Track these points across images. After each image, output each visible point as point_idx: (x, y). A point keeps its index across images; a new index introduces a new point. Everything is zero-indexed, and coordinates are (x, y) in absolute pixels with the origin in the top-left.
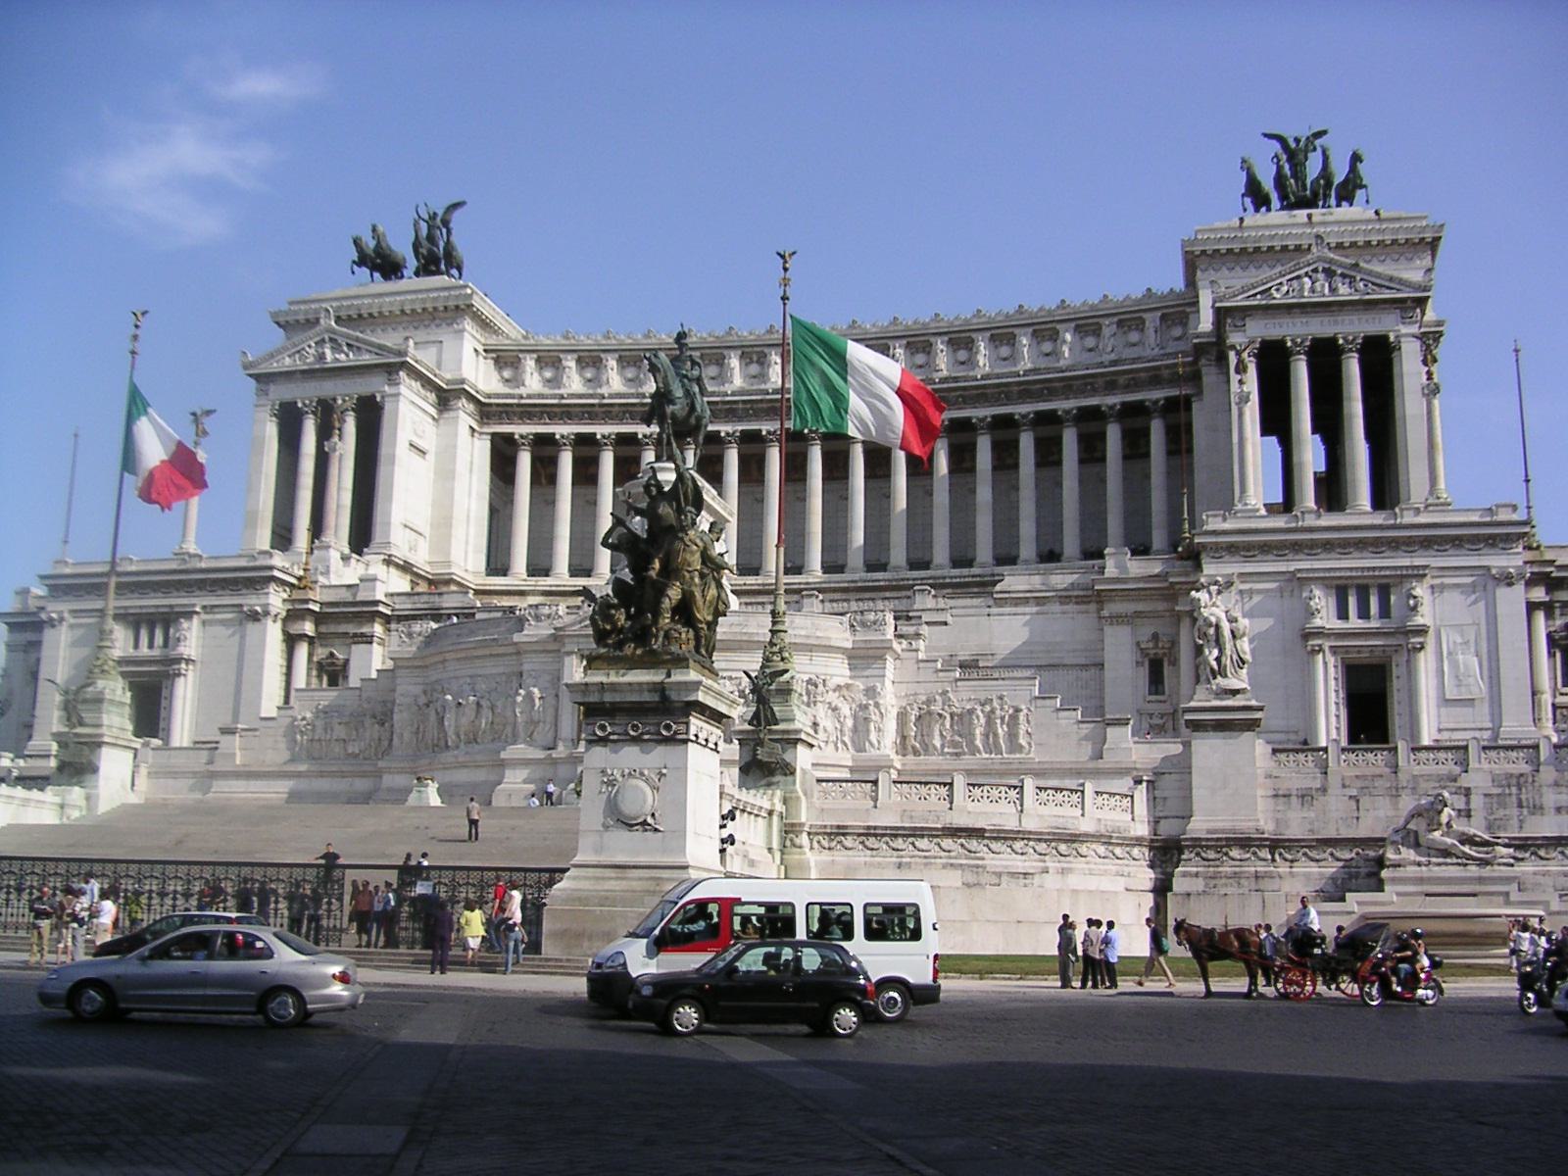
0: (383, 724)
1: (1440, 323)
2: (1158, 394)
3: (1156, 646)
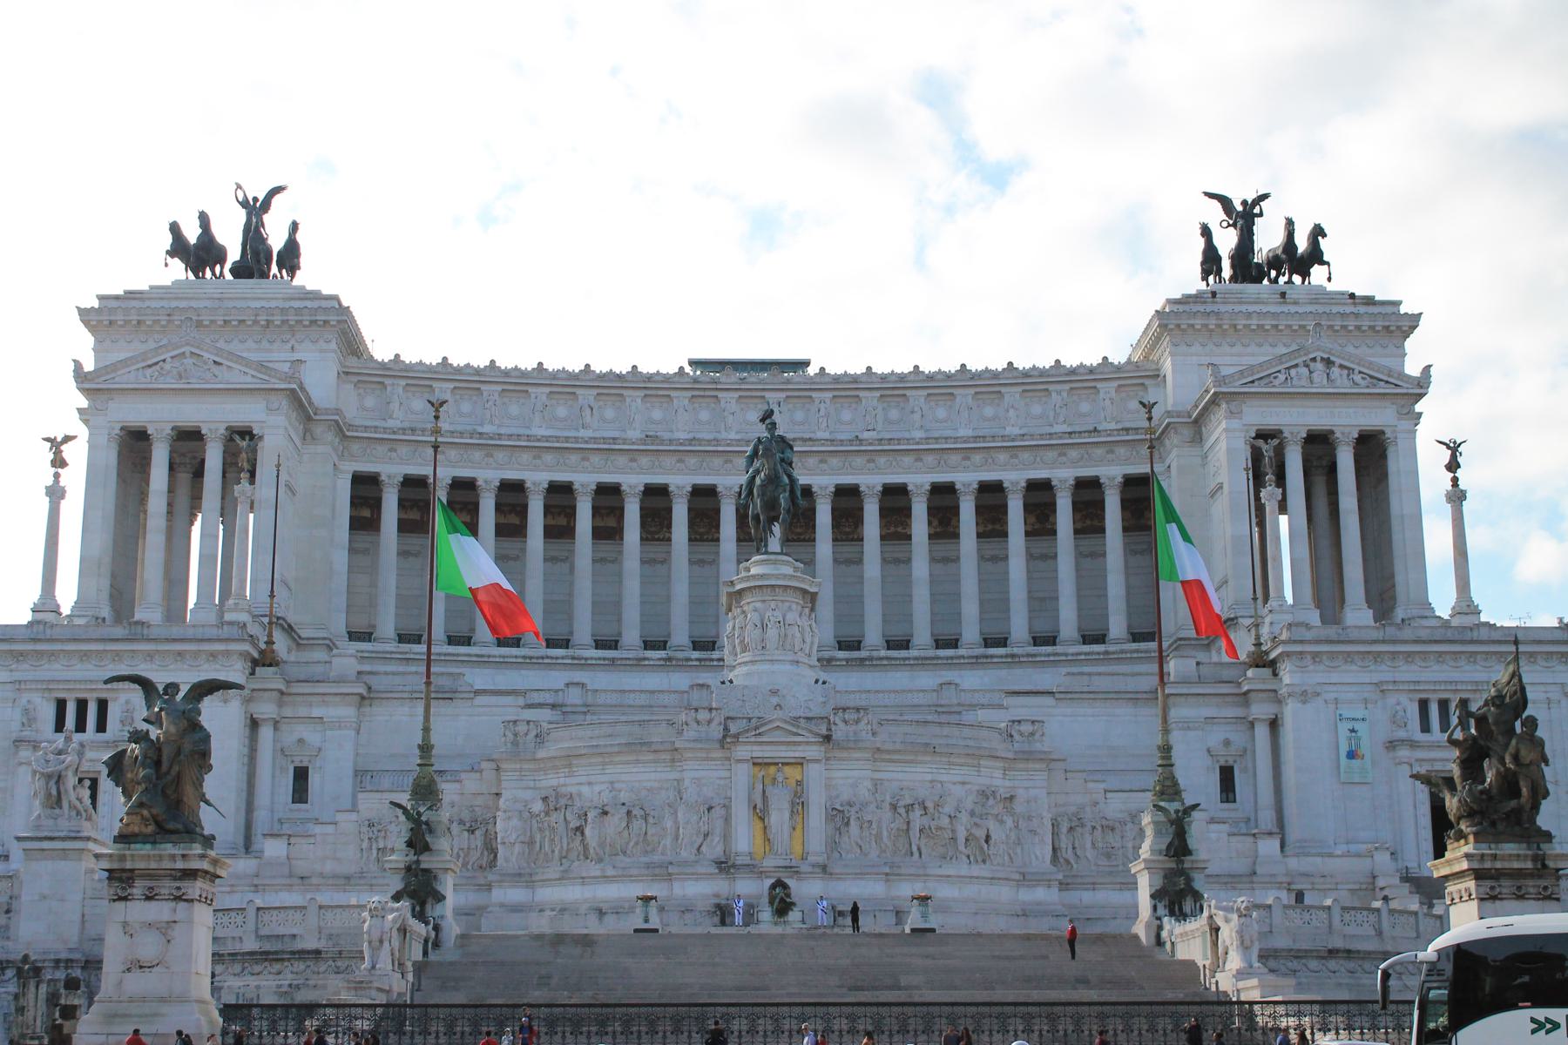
0: (472, 831)
1: (1420, 414)
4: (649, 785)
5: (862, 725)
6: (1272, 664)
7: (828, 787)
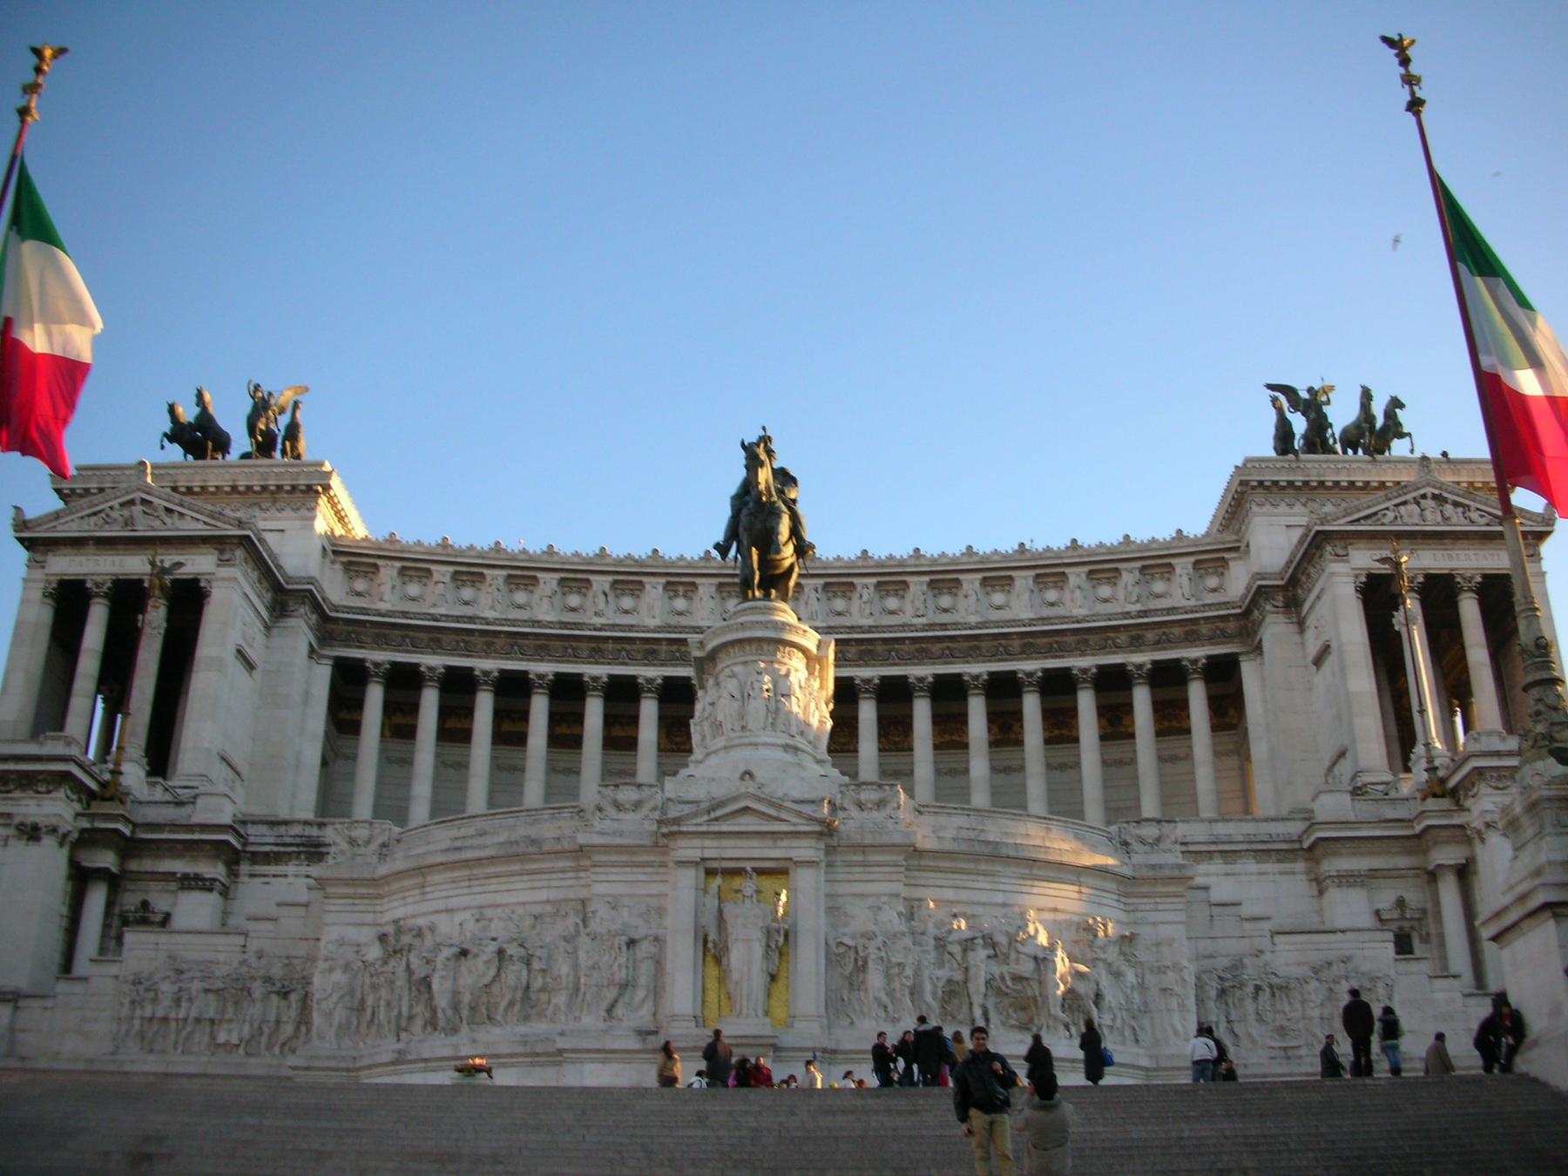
0: (284, 995)
2: (1198, 653)
3: (1403, 918)
4: (536, 909)
5: (888, 810)
6: (1453, 793)
7: (834, 910)
